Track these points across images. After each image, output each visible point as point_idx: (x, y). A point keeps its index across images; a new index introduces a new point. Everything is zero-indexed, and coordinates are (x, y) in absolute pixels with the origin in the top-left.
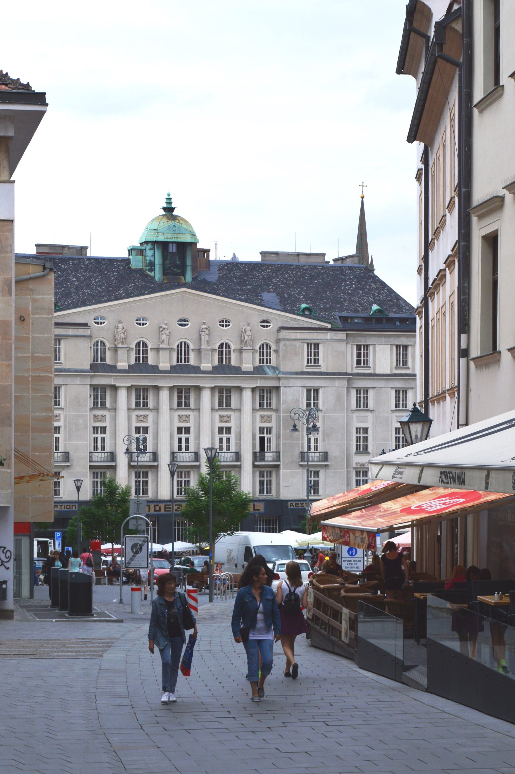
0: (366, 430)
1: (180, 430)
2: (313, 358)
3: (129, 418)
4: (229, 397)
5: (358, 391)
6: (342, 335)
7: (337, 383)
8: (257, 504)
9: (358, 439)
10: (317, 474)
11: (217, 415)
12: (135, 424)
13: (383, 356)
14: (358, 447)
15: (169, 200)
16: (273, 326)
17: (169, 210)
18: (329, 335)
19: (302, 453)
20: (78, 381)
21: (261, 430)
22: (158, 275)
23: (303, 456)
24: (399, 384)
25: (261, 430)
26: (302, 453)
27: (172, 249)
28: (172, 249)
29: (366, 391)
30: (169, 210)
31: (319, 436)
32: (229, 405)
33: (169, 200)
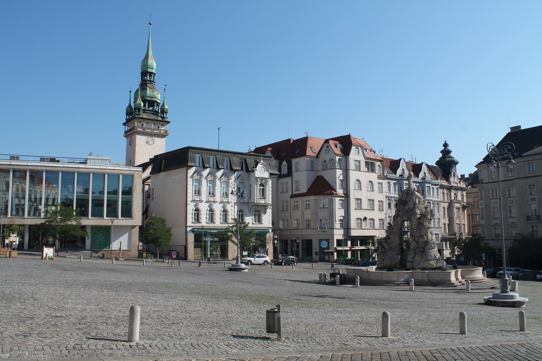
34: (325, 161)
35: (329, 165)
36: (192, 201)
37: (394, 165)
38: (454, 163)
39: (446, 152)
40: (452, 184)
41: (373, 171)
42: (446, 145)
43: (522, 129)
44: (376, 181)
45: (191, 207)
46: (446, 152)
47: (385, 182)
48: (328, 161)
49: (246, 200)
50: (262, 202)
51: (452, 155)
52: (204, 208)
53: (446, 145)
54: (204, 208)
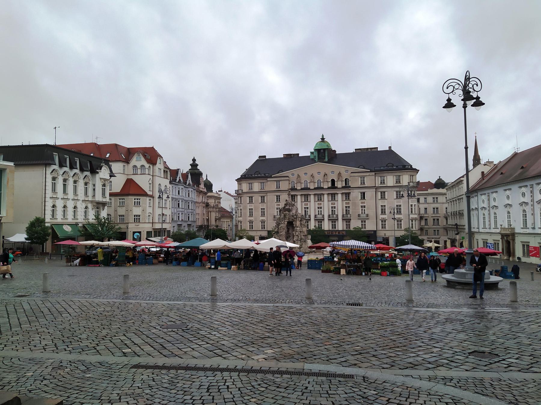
0: (385, 206)
1: (318, 208)
2: (363, 182)
3: (302, 205)
4: (335, 197)
5: (381, 193)
6: (373, 173)
7: (371, 190)
8: (343, 232)
9: (382, 209)
10: (365, 222)
11: (330, 203)
12: (304, 206)
13: (390, 180)
14: (382, 212)
15: (323, 136)
16: (349, 172)
17: (323, 139)
18: (368, 174)
19: (359, 215)
20: (285, 193)
21: (346, 207)
22: (316, 160)
23: (359, 215)
24: (398, 189)
25: (346, 207)
26: (359, 215)
27: (322, 151)
28: (322, 151)
29: (384, 192)
30: (323, 139)
31: (366, 209)
32: (335, 199)
33: (323, 136)
34: (135, 166)
35: (139, 172)
36: (51, 198)
37: (174, 173)
38: (201, 174)
39: (194, 165)
40: (201, 189)
41: (167, 178)
42: (194, 160)
43: (267, 158)
44: (169, 185)
45: (49, 204)
46: (194, 165)
47: (171, 186)
48: (139, 167)
49: (90, 199)
50: (104, 200)
51: (198, 167)
52: (60, 204)
53: (194, 160)
54: (60, 204)
